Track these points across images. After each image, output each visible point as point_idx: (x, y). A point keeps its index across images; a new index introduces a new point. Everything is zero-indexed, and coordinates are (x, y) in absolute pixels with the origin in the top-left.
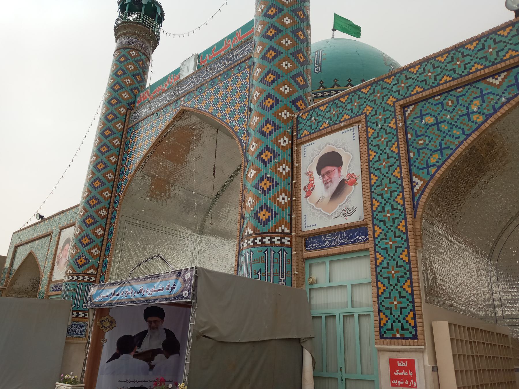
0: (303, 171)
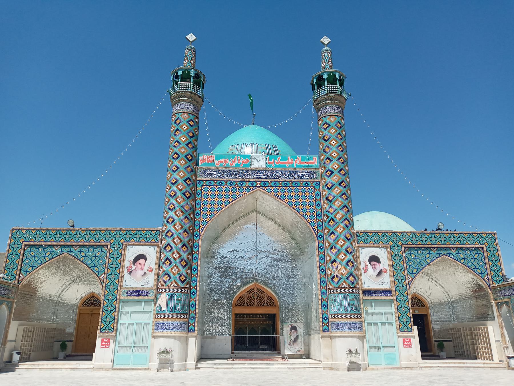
0: (362, 260)
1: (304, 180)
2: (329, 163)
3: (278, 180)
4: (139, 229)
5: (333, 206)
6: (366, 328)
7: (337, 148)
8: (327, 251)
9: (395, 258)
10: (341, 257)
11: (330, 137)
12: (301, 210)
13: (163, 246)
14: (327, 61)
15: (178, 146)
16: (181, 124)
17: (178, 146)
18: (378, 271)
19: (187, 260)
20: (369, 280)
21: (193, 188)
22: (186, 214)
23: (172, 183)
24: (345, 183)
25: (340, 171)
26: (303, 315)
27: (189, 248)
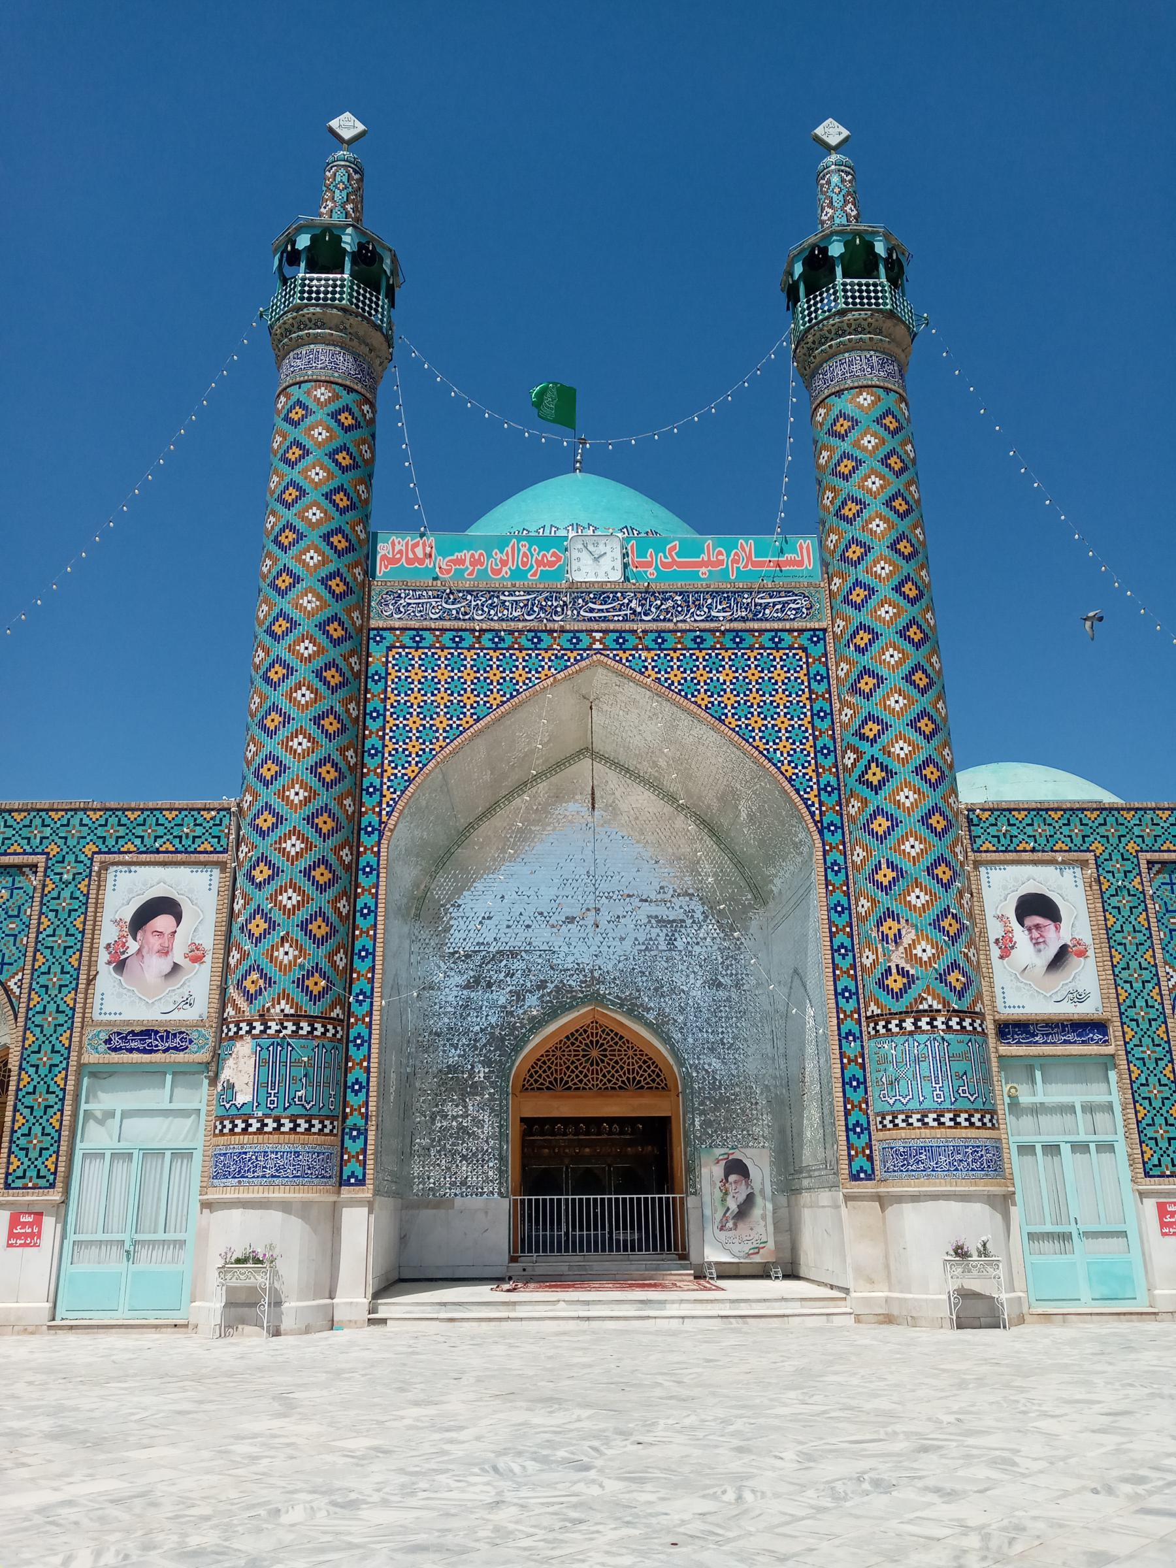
1: (768, 625)
2: (860, 559)
3: (671, 626)
4: (151, 805)
5: (877, 711)
6: (1015, 1162)
7: (888, 503)
8: (860, 881)
9: (1114, 901)
10: (912, 898)
11: (860, 463)
12: (757, 734)
13: (240, 865)
14: (838, 200)
15: (295, 501)
16: (309, 421)
17: (295, 501)
18: (1051, 951)
19: (334, 918)
20: (1019, 983)
21: (352, 653)
22: (328, 748)
23: (272, 634)
24: (919, 627)
25: (902, 584)
26: (767, 1119)
27: (340, 871)
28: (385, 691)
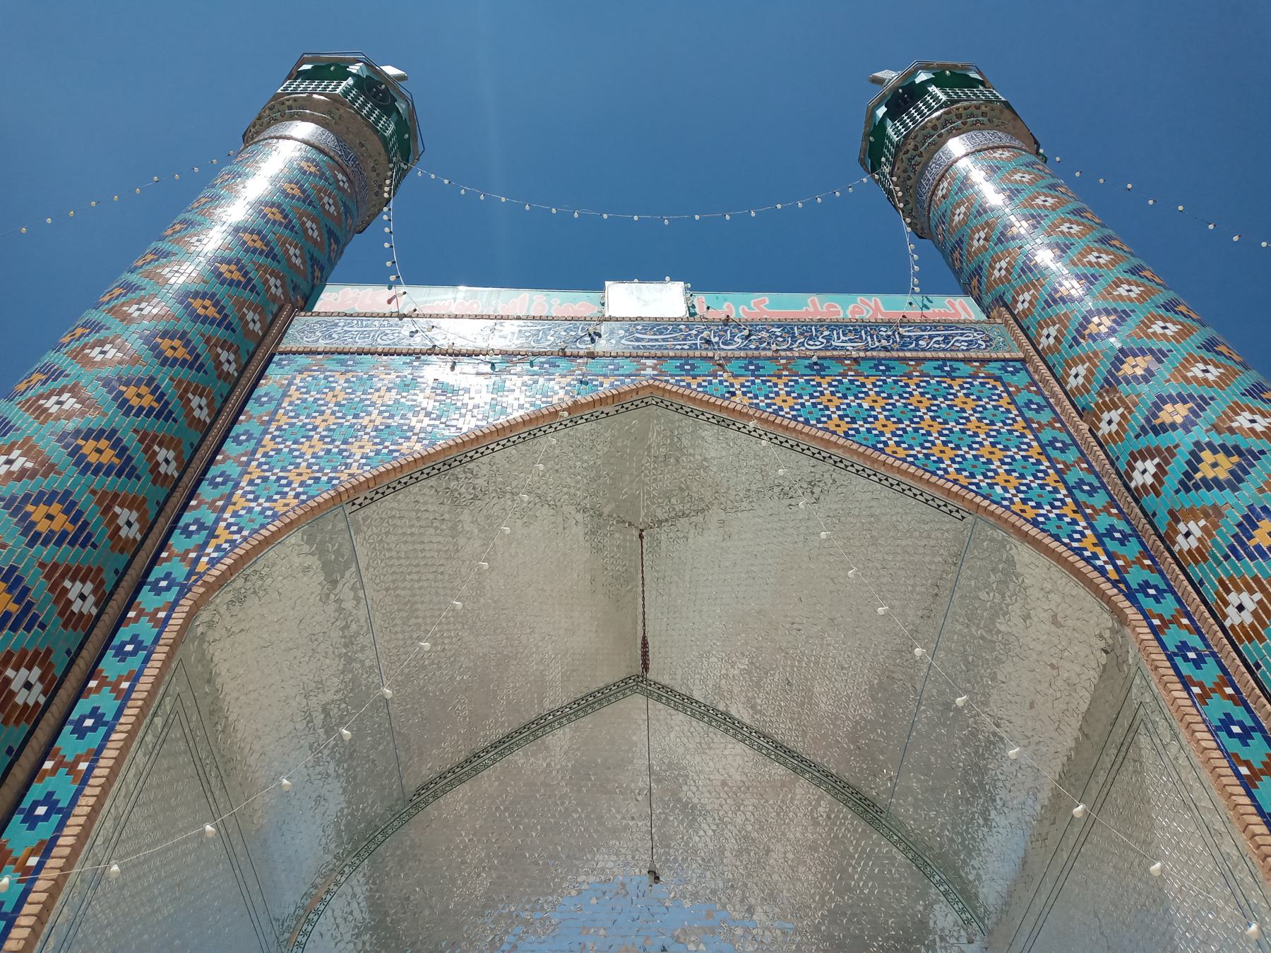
28: (275, 412)
